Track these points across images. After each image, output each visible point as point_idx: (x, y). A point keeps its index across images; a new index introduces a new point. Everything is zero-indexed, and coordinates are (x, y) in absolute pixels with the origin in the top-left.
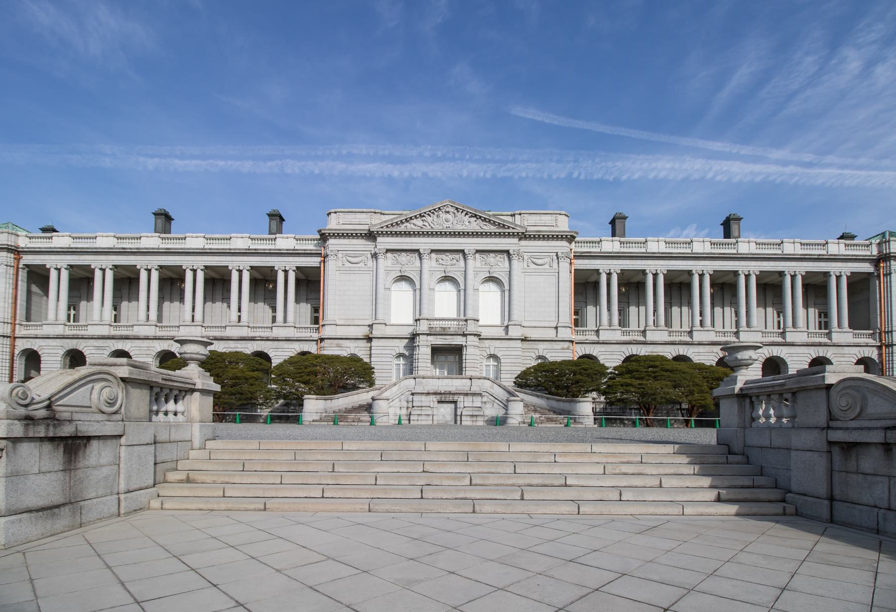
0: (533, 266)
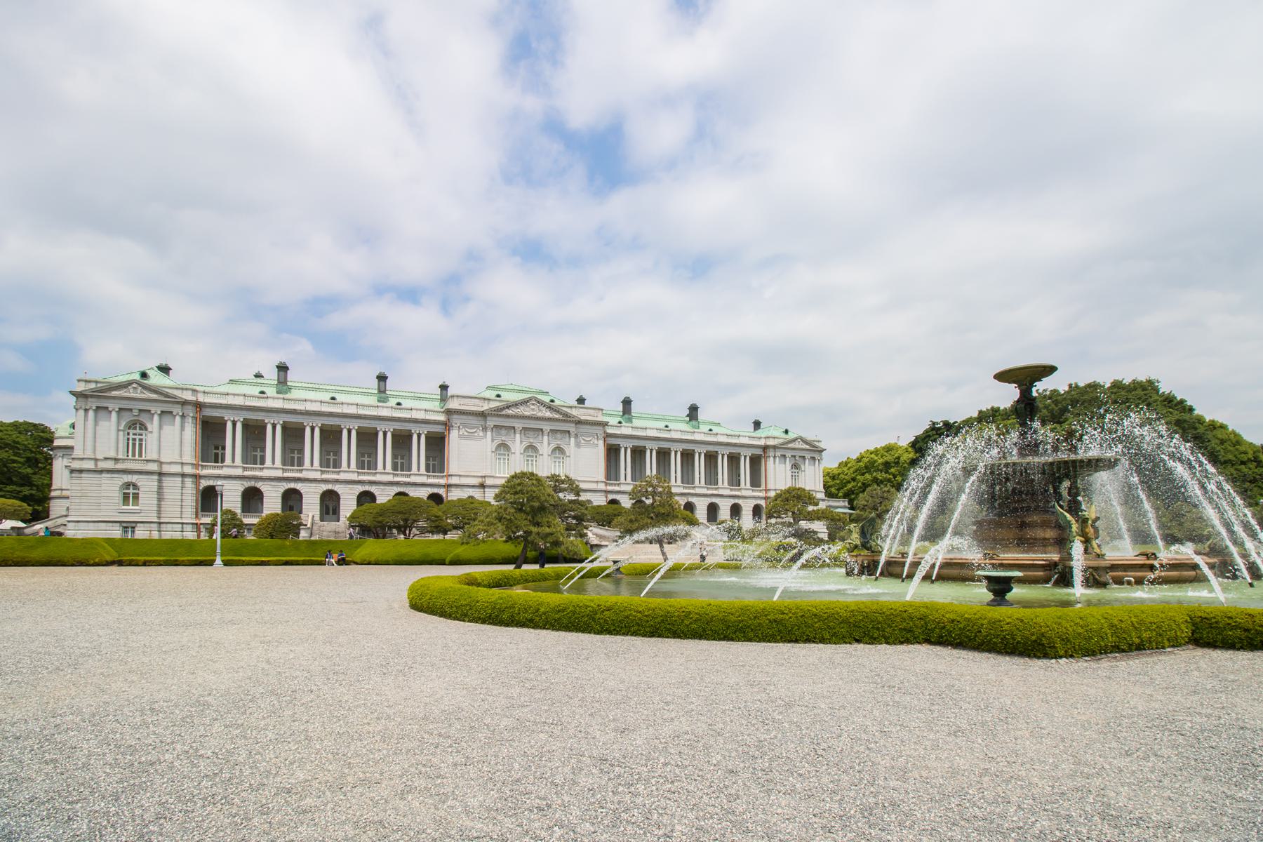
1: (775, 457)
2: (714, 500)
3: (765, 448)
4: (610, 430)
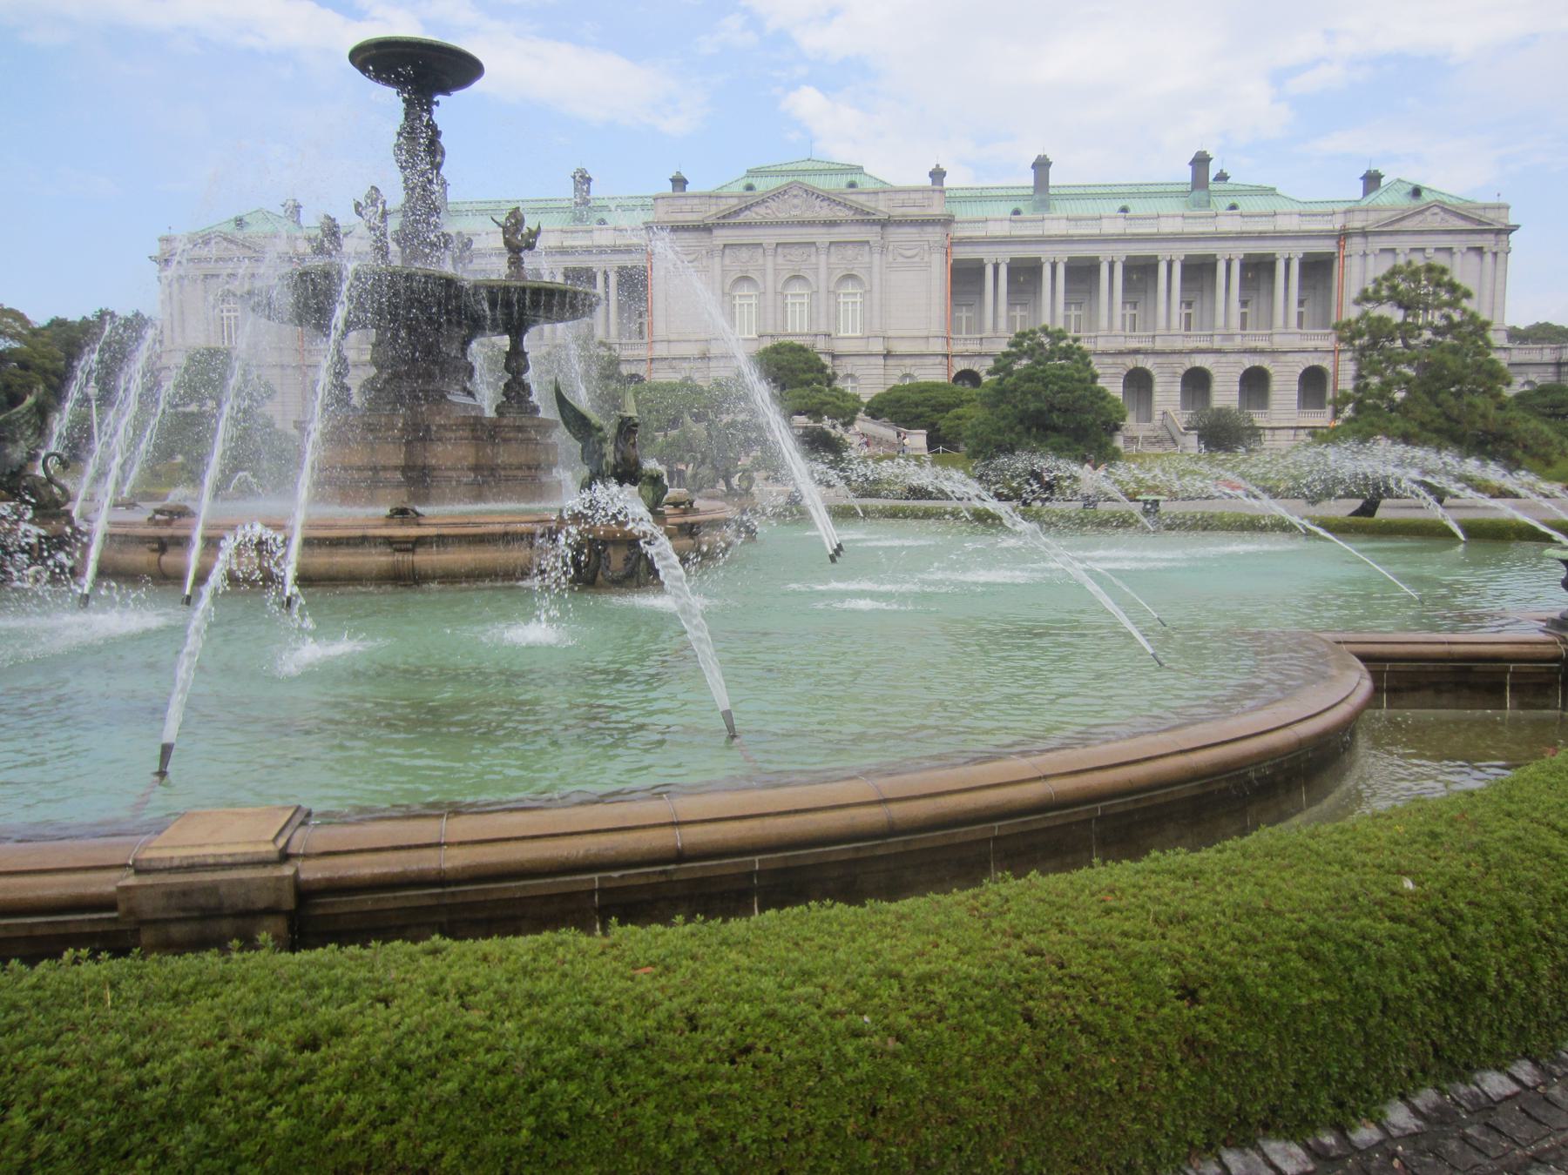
0: (900, 259)
1: (1365, 255)
2: (1199, 361)
3: (1343, 235)
4: (959, 232)
